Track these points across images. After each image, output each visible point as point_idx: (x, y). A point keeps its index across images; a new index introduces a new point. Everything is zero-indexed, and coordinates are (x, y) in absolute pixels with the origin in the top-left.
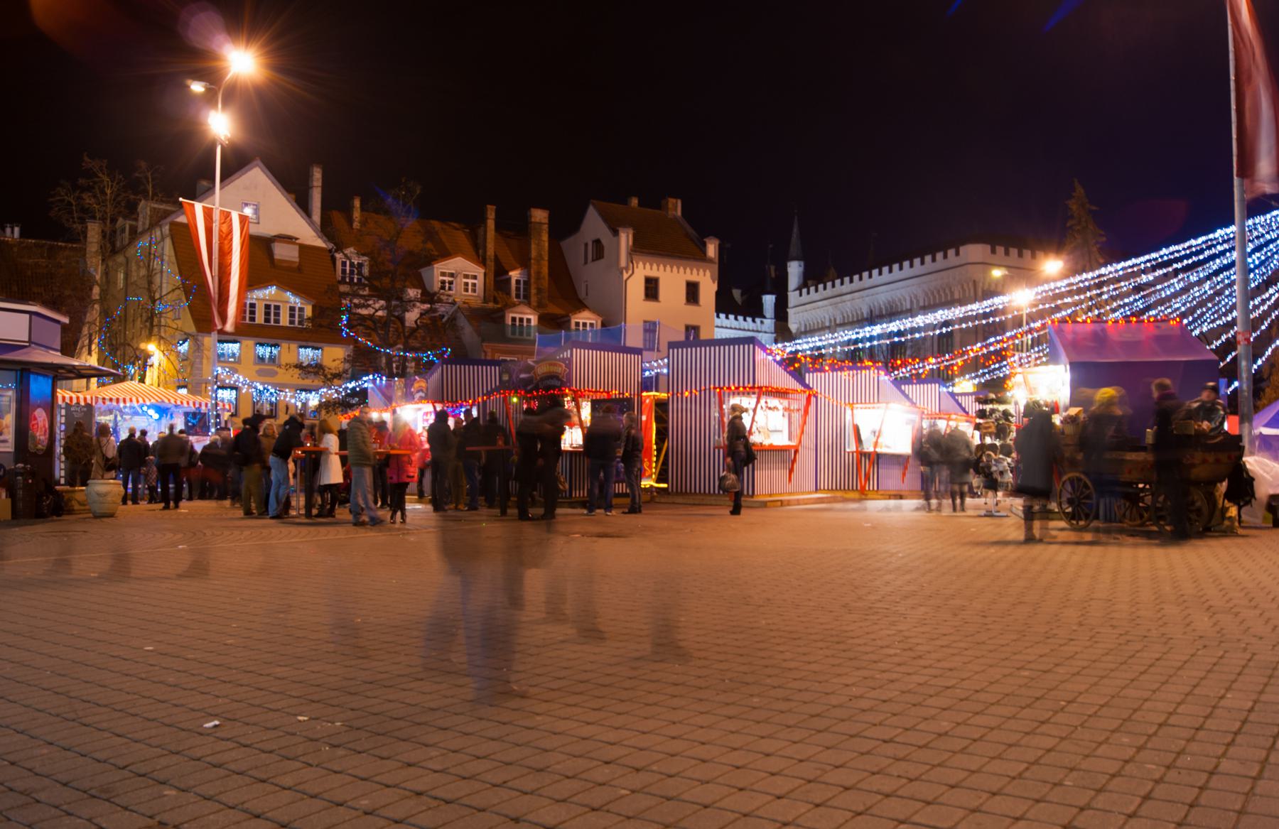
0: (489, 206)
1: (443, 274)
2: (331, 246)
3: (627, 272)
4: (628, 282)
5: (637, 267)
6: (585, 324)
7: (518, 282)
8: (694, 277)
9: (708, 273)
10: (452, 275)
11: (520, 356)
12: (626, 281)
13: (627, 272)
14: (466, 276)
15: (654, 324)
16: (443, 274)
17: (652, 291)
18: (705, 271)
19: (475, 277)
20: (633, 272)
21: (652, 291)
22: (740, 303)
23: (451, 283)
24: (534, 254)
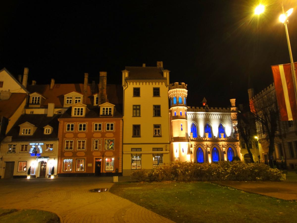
0: (85, 74)
1: (68, 98)
2: (28, 92)
3: (125, 87)
4: (125, 91)
5: (130, 85)
6: (107, 109)
7: (97, 98)
8: (157, 85)
9: (164, 84)
10: (71, 98)
11: (75, 123)
12: (124, 90)
13: (125, 87)
14: (76, 98)
15: (139, 106)
16: (68, 98)
17: (137, 92)
18: (162, 83)
19: (80, 98)
20: (128, 87)
21: (137, 92)
22: (204, 98)
23: (70, 101)
24: (100, 87)
